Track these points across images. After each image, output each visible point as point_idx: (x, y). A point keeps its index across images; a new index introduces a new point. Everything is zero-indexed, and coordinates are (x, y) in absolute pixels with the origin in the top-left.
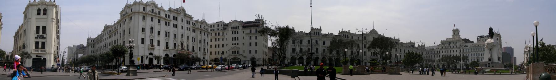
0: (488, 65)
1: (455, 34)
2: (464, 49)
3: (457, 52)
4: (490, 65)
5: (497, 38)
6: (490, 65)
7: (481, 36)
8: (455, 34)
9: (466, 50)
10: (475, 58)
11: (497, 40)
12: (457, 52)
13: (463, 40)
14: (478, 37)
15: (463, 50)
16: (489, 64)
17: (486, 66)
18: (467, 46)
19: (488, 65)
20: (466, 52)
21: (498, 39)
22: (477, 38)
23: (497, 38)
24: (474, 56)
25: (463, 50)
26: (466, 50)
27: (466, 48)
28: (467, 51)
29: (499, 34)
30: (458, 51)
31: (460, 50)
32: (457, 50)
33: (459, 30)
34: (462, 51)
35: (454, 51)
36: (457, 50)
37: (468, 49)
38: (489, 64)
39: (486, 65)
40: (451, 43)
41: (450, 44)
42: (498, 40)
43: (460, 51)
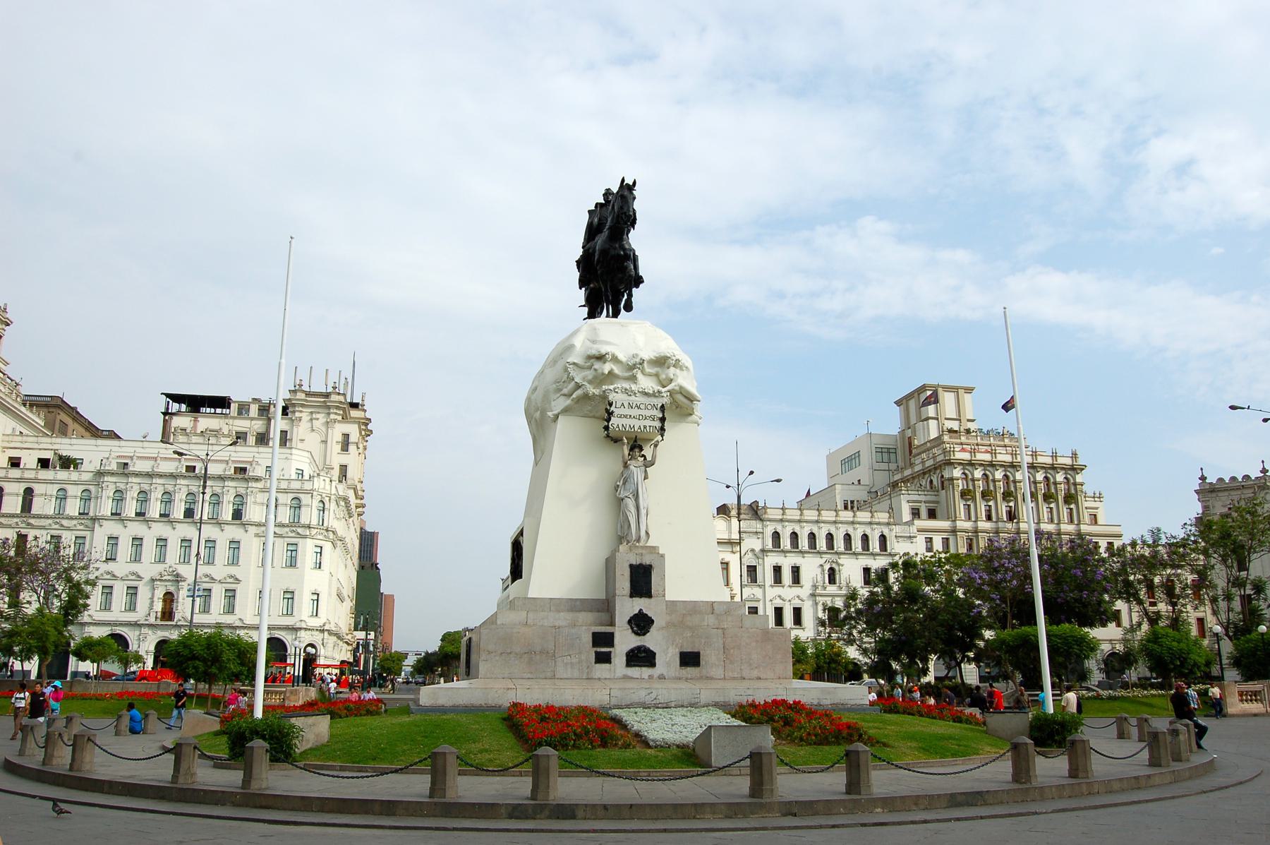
0: (625, 640)
2: (38, 489)
4: (651, 640)
5: (346, 436)
6: (651, 640)
7: (195, 403)
9: (62, 497)
10: (140, 578)
13: (34, 403)
14: (175, 407)
16: (641, 623)
17: (604, 658)
18: (67, 463)
20: (60, 515)
21: (354, 437)
22: (165, 414)
23: (346, 436)
24: (137, 558)
26: (62, 497)
27: (62, 475)
28: (73, 508)
29: (354, 406)
37: (75, 491)
39: (603, 640)
42: (352, 448)
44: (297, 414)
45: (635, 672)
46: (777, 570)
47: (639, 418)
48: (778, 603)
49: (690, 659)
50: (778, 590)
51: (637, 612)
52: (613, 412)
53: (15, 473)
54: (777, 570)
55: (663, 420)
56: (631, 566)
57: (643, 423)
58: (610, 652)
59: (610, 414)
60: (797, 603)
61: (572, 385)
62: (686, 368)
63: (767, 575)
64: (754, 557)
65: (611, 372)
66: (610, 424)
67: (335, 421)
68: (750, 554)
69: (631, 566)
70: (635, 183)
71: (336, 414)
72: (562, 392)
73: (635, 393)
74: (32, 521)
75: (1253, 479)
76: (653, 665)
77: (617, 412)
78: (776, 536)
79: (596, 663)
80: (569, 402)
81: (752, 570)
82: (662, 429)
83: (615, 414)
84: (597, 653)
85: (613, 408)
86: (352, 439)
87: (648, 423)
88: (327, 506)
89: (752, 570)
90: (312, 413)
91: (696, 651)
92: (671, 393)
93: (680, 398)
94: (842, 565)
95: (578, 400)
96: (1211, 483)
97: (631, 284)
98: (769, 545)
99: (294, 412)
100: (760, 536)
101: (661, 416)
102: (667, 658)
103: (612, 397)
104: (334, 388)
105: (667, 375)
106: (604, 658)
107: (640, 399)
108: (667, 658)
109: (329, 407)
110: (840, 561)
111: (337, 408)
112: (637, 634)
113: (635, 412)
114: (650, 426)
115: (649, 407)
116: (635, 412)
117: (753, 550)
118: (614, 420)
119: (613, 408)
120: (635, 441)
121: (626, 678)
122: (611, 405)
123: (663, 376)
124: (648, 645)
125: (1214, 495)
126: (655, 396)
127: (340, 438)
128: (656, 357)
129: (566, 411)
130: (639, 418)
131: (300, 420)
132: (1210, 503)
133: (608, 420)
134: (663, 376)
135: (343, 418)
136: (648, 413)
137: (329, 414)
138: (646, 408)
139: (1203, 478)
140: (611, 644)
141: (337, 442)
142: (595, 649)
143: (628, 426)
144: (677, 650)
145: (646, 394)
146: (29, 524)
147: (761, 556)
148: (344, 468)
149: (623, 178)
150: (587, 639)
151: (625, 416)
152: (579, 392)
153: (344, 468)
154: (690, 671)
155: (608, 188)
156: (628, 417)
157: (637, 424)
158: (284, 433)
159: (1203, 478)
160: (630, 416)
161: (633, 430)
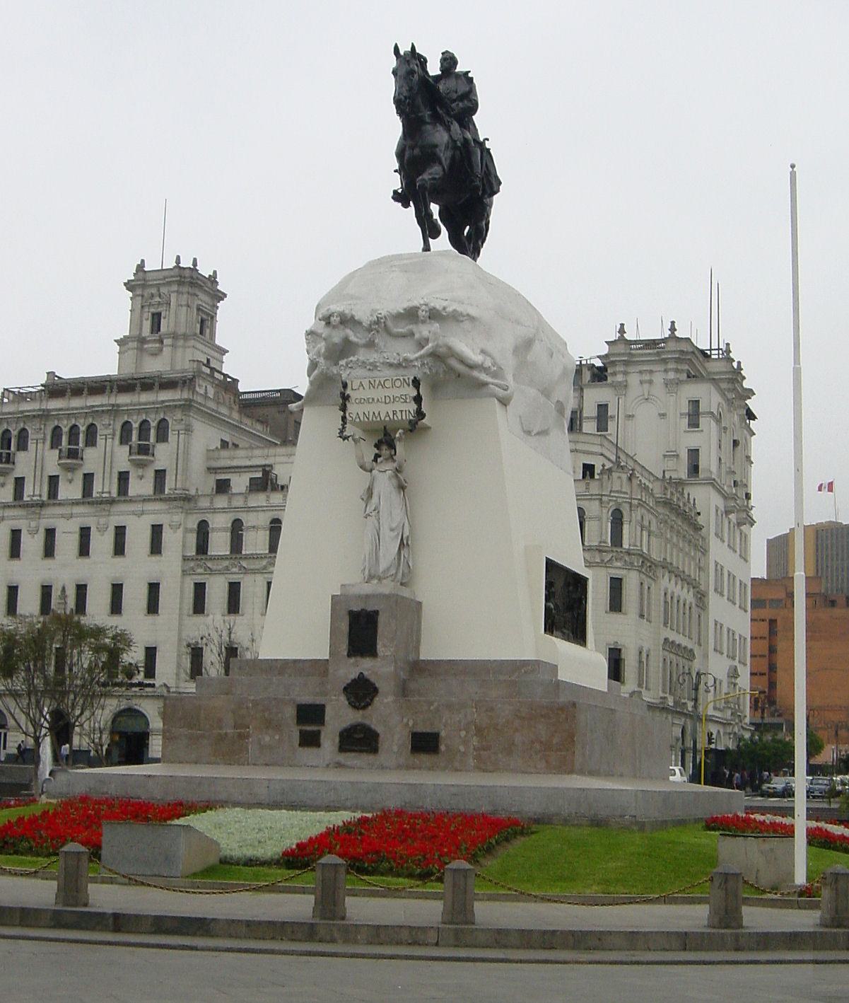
1: (156, 327)
2: (248, 519)
3: (156, 547)
5: (695, 404)
8: (156, 327)
11: (694, 423)
12: (156, 547)
15: (237, 528)
16: (361, 692)
17: (310, 740)
19: (340, 715)
23: (695, 404)
25: (237, 528)
30: (177, 542)
31: (203, 531)
32: (157, 530)
33: (213, 279)
34: (219, 543)
35: (120, 532)
36: (157, 530)
38: (361, 692)
39: (311, 715)
40: (92, 431)
41: (73, 454)
42: (703, 421)
43: (202, 547)
44: (620, 378)
45: (350, 759)
47: (387, 401)
49: (425, 743)
51: (353, 675)
52: (349, 396)
53: (221, 502)
55: (418, 399)
56: (351, 613)
57: (389, 409)
58: (319, 732)
59: (345, 398)
62: (468, 315)
65: (346, 341)
66: (347, 415)
67: (679, 383)
69: (351, 613)
70: (413, 47)
71: (677, 371)
73: (376, 367)
74: (244, 564)
76: (374, 750)
79: (300, 745)
82: (420, 414)
83: (352, 399)
84: (301, 732)
85: (348, 392)
86: (703, 407)
87: (399, 406)
88: (625, 518)
90: (641, 372)
91: (436, 730)
92: (434, 355)
93: (453, 363)
97: (424, 199)
99: (614, 374)
101: (415, 393)
102: (394, 738)
104: (673, 329)
105: (420, 332)
106: (310, 740)
108: (394, 738)
109: (665, 361)
111: (678, 360)
112: (355, 707)
113: (379, 393)
114: (402, 411)
115: (398, 383)
118: (352, 408)
119: (348, 392)
120: (386, 433)
121: (339, 765)
122: (345, 386)
124: (367, 722)
126: (405, 367)
127: (685, 409)
128: (405, 309)
130: (387, 401)
131: (626, 386)
133: (344, 408)
135: (688, 377)
136: (397, 392)
137: (666, 371)
138: (393, 385)
140: (321, 721)
141: (681, 414)
142: (300, 727)
143: (371, 414)
144: (408, 730)
145: (391, 365)
146: (241, 567)
148: (694, 454)
149: (396, 45)
150: (290, 712)
151: (367, 401)
153: (694, 454)
154: (425, 758)
155: (444, 51)
156: (371, 401)
158: (603, 408)
160: (373, 399)
161: (379, 419)
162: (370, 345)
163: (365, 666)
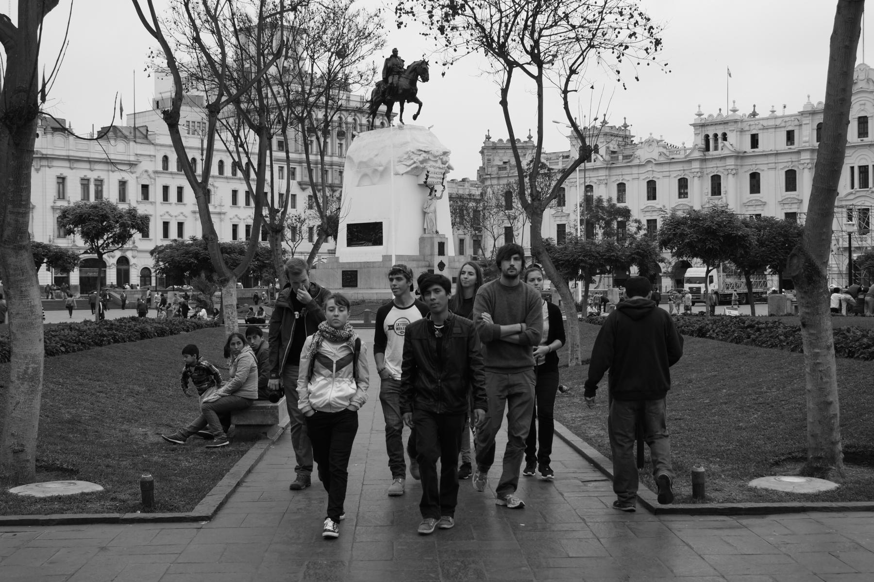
46: (166, 189)
48: (167, 218)
50: (166, 208)
54: (166, 189)
60: (181, 219)
61: (412, 162)
63: (156, 193)
64: (148, 177)
68: (145, 176)
72: (405, 163)
75: (522, 141)
77: (430, 175)
78: (166, 159)
80: (409, 169)
81: (145, 188)
87: (439, 180)
89: (145, 188)
94: (217, 188)
95: (412, 169)
96: (493, 143)
98: (160, 168)
100: (153, 159)
103: (429, 169)
107: (438, 170)
110: (216, 184)
113: (435, 176)
116: (435, 176)
117: (146, 171)
118: (429, 179)
122: (428, 172)
123: (444, 160)
125: (495, 151)
129: (407, 173)
132: (491, 157)
133: (426, 179)
134: (444, 160)
139: (488, 138)
145: (440, 168)
147: (153, 175)
152: (414, 165)
157: (435, 180)
159: (488, 138)
162: (436, 161)
163: (441, 258)
